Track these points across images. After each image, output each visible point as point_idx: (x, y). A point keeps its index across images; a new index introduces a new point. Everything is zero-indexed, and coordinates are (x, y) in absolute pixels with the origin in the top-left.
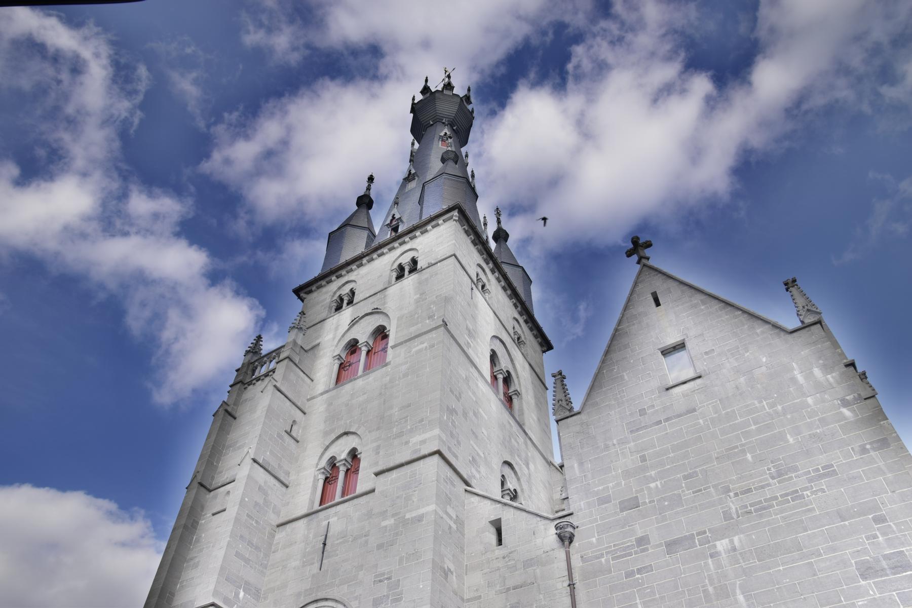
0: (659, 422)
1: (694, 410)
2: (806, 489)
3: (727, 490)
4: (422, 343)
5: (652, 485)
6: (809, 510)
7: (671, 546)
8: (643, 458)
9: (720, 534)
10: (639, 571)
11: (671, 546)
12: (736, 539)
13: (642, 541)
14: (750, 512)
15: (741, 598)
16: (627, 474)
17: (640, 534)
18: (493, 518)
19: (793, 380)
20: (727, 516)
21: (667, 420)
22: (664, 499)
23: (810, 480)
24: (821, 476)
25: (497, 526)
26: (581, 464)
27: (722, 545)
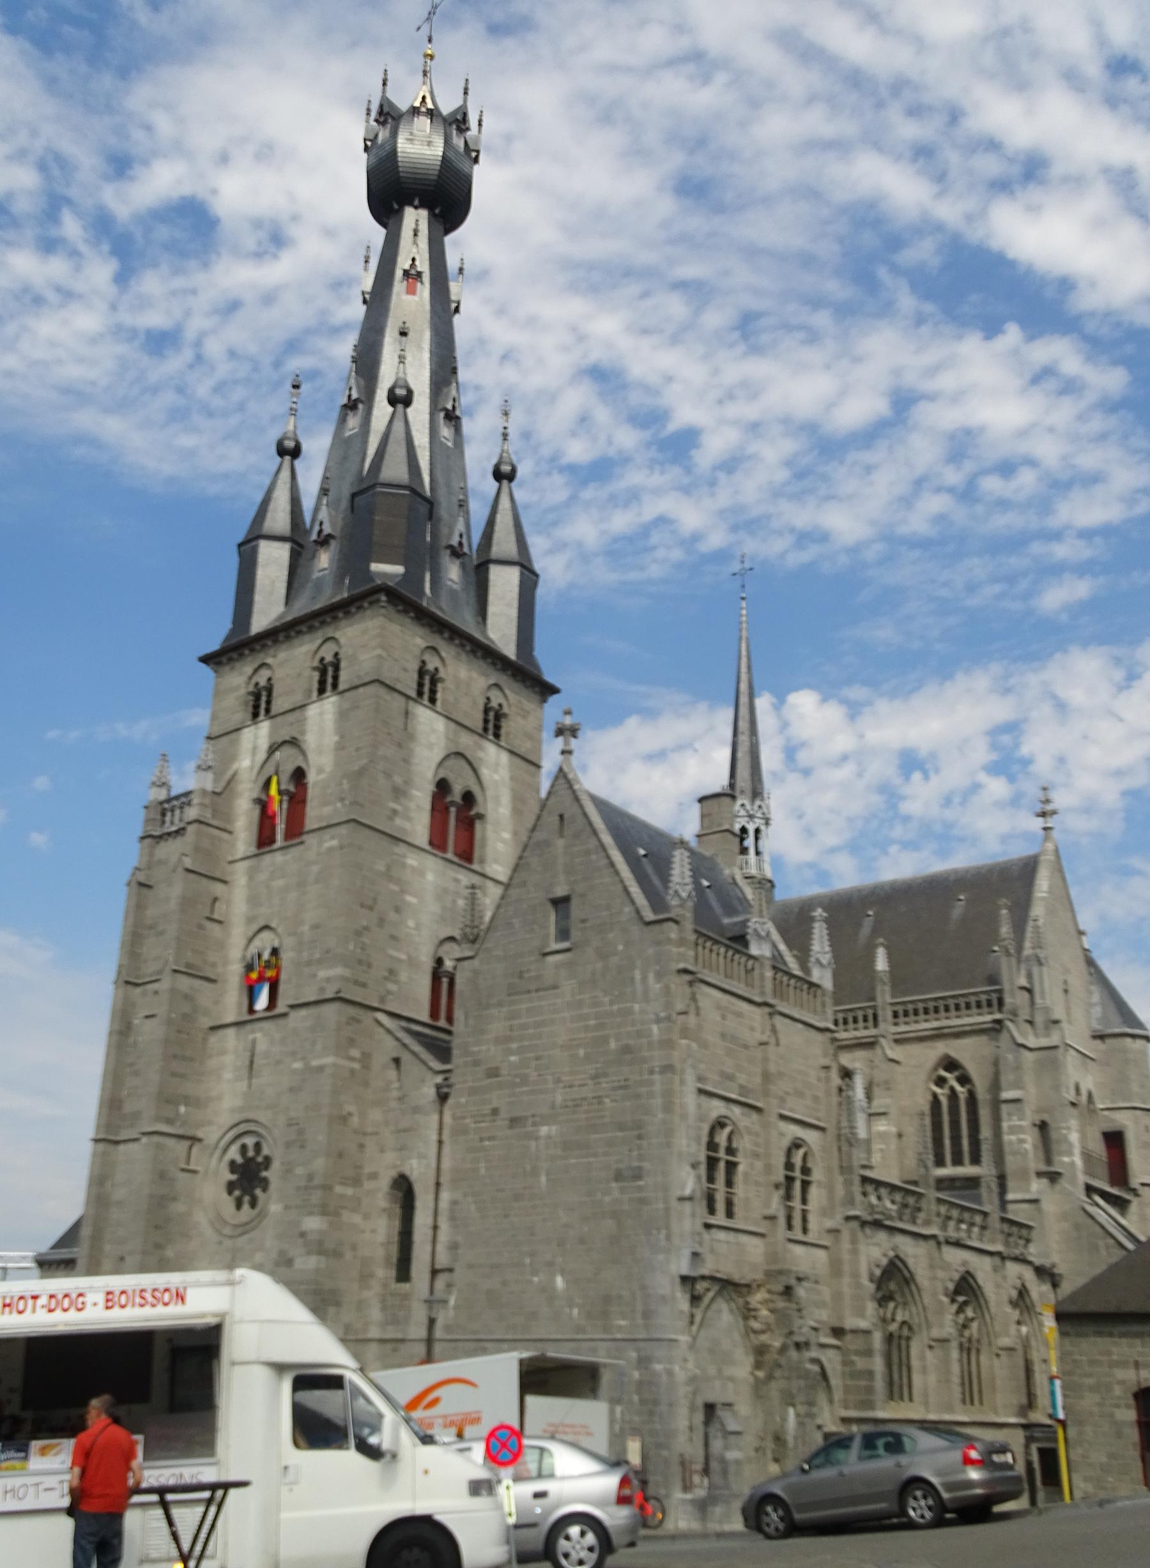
0: (529, 992)
1: (555, 987)
2: (606, 1097)
3: (559, 1081)
4: (333, 838)
5: (513, 1058)
6: (603, 1117)
7: (514, 1122)
8: (511, 1028)
9: (546, 1120)
10: (490, 1139)
11: (514, 1122)
12: (554, 1128)
13: (495, 1112)
14: (567, 1107)
15: (543, 1179)
16: (498, 1041)
17: (495, 1105)
18: (395, 1055)
19: (632, 979)
20: (553, 1107)
21: (537, 990)
22: (516, 1076)
23: (614, 1089)
24: (621, 1087)
25: (397, 1061)
26: (466, 1017)
27: (544, 1130)
